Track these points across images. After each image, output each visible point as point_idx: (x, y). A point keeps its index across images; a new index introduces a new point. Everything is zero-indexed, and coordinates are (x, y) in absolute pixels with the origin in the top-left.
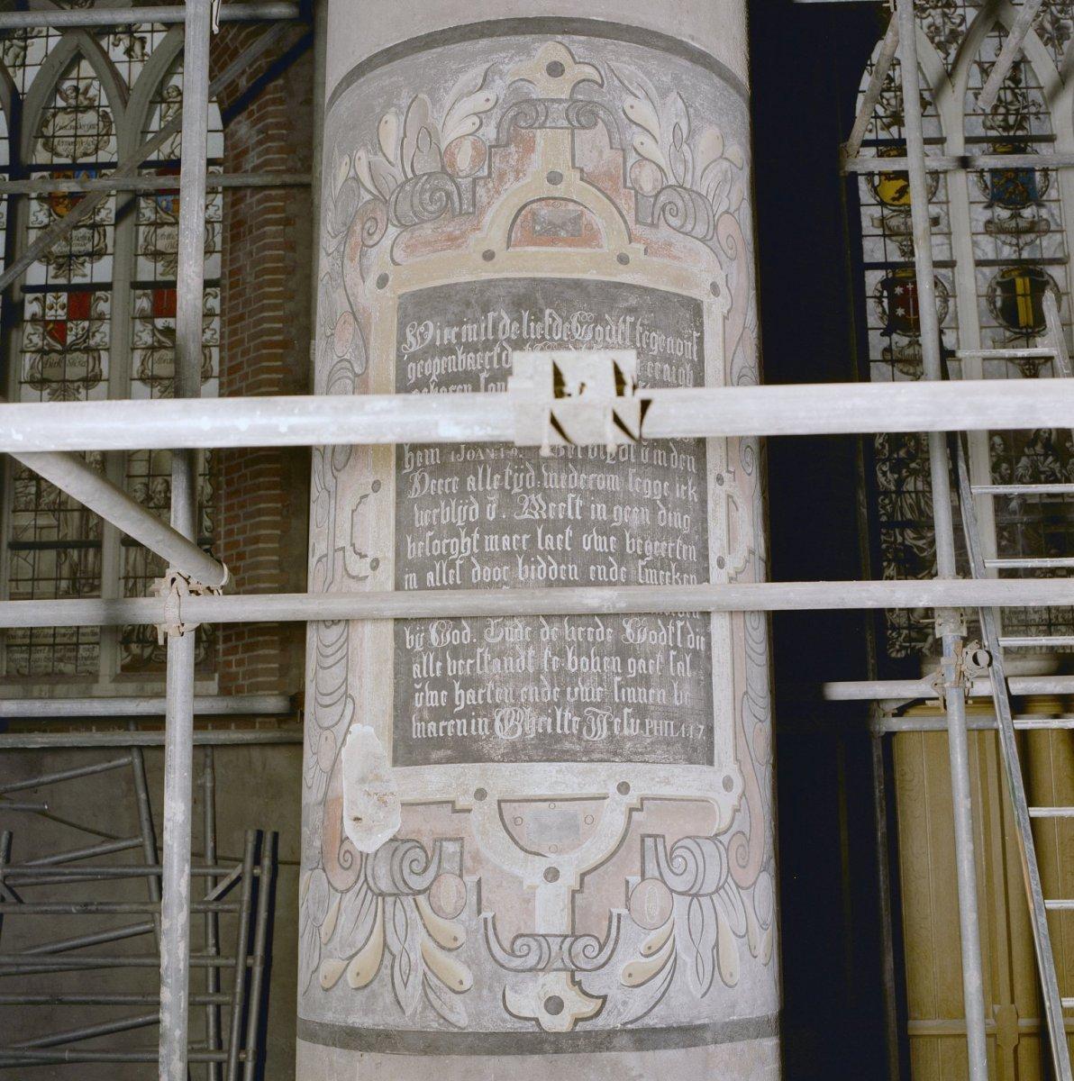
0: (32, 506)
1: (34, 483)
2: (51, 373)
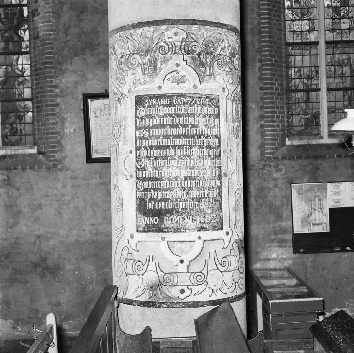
0: (333, 76)
1: (333, 67)
2: (336, 27)
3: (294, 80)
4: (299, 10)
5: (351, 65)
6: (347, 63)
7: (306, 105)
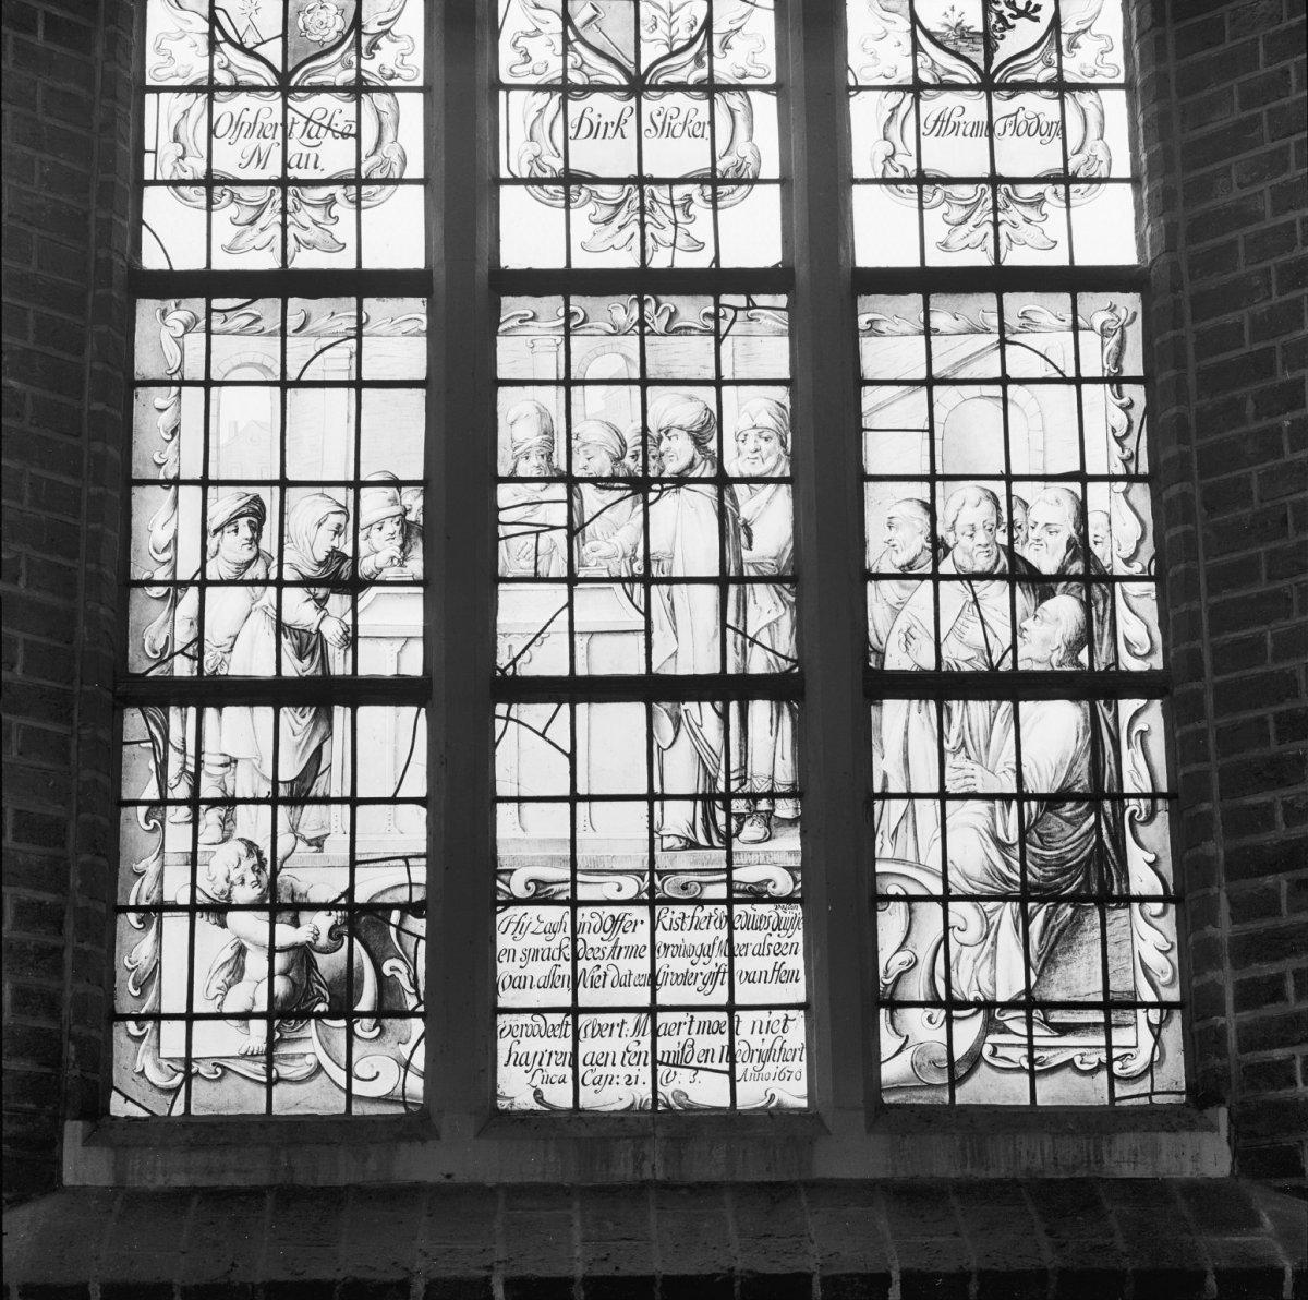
1: (559, 490)
3: (193, 592)
6: (691, 466)
7: (294, 830)
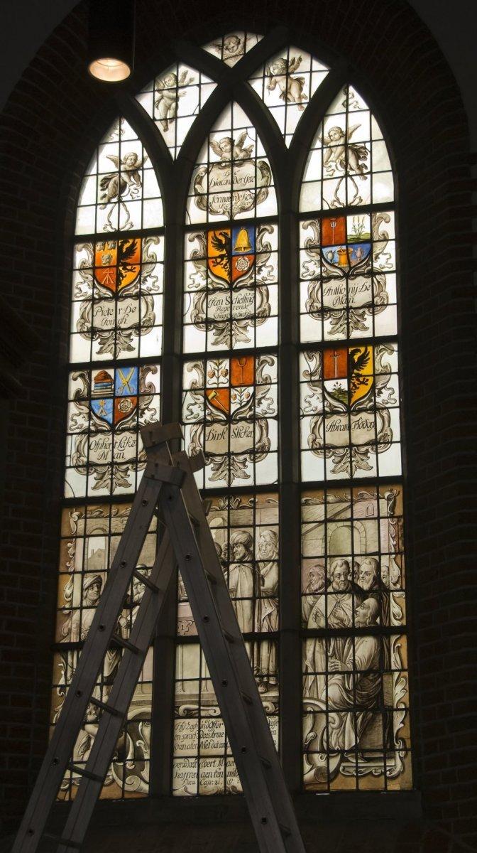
4: (109, 403)
5: (254, 563)
6: (244, 556)
